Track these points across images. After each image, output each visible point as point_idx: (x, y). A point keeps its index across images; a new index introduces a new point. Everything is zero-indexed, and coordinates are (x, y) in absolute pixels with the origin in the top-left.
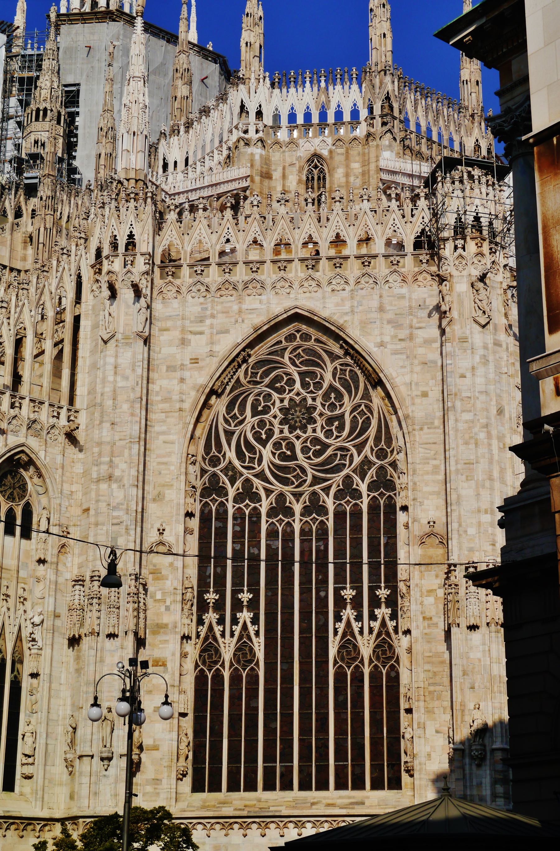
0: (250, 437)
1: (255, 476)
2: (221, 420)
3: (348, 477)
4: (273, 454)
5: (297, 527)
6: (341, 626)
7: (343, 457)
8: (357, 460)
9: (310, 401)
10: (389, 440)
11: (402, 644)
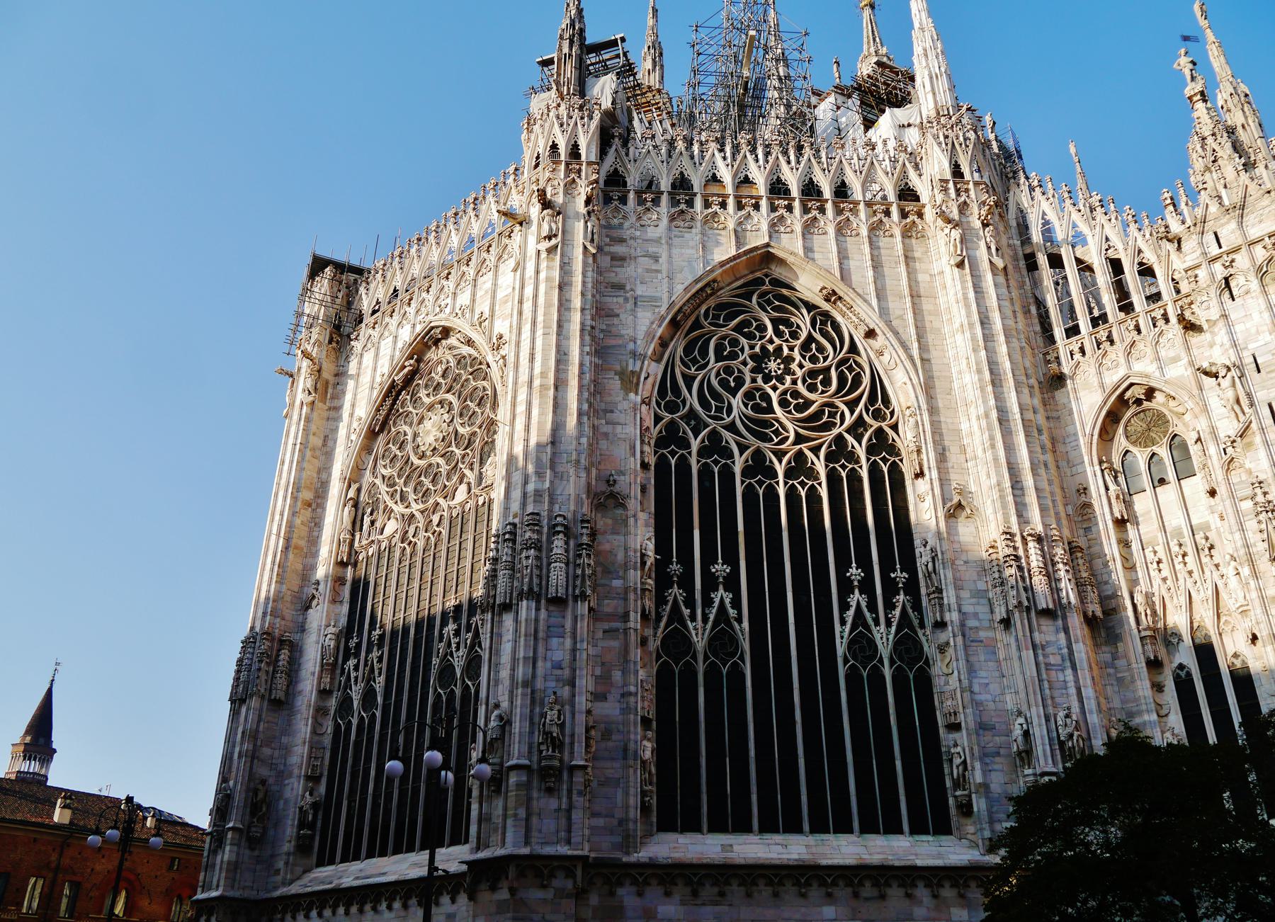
0: (715, 383)
1: (725, 427)
2: (678, 362)
3: (840, 436)
4: (746, 405)
5: (781, 491)
6: (850, 614)
7: (832, 415)
8: (849, 420)
9: (786, 351)
10: (886, 401)
11: (928, 641)
